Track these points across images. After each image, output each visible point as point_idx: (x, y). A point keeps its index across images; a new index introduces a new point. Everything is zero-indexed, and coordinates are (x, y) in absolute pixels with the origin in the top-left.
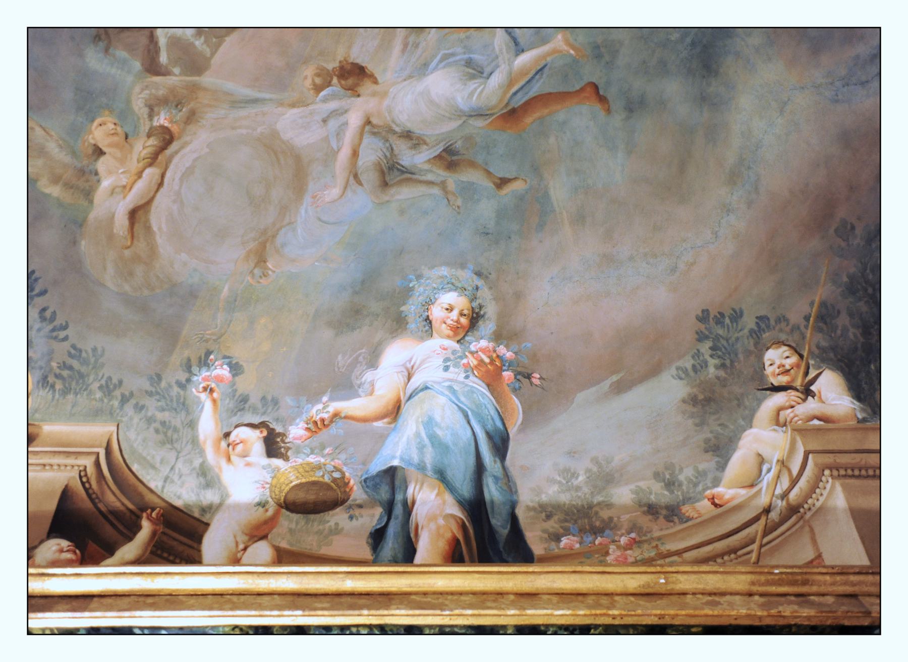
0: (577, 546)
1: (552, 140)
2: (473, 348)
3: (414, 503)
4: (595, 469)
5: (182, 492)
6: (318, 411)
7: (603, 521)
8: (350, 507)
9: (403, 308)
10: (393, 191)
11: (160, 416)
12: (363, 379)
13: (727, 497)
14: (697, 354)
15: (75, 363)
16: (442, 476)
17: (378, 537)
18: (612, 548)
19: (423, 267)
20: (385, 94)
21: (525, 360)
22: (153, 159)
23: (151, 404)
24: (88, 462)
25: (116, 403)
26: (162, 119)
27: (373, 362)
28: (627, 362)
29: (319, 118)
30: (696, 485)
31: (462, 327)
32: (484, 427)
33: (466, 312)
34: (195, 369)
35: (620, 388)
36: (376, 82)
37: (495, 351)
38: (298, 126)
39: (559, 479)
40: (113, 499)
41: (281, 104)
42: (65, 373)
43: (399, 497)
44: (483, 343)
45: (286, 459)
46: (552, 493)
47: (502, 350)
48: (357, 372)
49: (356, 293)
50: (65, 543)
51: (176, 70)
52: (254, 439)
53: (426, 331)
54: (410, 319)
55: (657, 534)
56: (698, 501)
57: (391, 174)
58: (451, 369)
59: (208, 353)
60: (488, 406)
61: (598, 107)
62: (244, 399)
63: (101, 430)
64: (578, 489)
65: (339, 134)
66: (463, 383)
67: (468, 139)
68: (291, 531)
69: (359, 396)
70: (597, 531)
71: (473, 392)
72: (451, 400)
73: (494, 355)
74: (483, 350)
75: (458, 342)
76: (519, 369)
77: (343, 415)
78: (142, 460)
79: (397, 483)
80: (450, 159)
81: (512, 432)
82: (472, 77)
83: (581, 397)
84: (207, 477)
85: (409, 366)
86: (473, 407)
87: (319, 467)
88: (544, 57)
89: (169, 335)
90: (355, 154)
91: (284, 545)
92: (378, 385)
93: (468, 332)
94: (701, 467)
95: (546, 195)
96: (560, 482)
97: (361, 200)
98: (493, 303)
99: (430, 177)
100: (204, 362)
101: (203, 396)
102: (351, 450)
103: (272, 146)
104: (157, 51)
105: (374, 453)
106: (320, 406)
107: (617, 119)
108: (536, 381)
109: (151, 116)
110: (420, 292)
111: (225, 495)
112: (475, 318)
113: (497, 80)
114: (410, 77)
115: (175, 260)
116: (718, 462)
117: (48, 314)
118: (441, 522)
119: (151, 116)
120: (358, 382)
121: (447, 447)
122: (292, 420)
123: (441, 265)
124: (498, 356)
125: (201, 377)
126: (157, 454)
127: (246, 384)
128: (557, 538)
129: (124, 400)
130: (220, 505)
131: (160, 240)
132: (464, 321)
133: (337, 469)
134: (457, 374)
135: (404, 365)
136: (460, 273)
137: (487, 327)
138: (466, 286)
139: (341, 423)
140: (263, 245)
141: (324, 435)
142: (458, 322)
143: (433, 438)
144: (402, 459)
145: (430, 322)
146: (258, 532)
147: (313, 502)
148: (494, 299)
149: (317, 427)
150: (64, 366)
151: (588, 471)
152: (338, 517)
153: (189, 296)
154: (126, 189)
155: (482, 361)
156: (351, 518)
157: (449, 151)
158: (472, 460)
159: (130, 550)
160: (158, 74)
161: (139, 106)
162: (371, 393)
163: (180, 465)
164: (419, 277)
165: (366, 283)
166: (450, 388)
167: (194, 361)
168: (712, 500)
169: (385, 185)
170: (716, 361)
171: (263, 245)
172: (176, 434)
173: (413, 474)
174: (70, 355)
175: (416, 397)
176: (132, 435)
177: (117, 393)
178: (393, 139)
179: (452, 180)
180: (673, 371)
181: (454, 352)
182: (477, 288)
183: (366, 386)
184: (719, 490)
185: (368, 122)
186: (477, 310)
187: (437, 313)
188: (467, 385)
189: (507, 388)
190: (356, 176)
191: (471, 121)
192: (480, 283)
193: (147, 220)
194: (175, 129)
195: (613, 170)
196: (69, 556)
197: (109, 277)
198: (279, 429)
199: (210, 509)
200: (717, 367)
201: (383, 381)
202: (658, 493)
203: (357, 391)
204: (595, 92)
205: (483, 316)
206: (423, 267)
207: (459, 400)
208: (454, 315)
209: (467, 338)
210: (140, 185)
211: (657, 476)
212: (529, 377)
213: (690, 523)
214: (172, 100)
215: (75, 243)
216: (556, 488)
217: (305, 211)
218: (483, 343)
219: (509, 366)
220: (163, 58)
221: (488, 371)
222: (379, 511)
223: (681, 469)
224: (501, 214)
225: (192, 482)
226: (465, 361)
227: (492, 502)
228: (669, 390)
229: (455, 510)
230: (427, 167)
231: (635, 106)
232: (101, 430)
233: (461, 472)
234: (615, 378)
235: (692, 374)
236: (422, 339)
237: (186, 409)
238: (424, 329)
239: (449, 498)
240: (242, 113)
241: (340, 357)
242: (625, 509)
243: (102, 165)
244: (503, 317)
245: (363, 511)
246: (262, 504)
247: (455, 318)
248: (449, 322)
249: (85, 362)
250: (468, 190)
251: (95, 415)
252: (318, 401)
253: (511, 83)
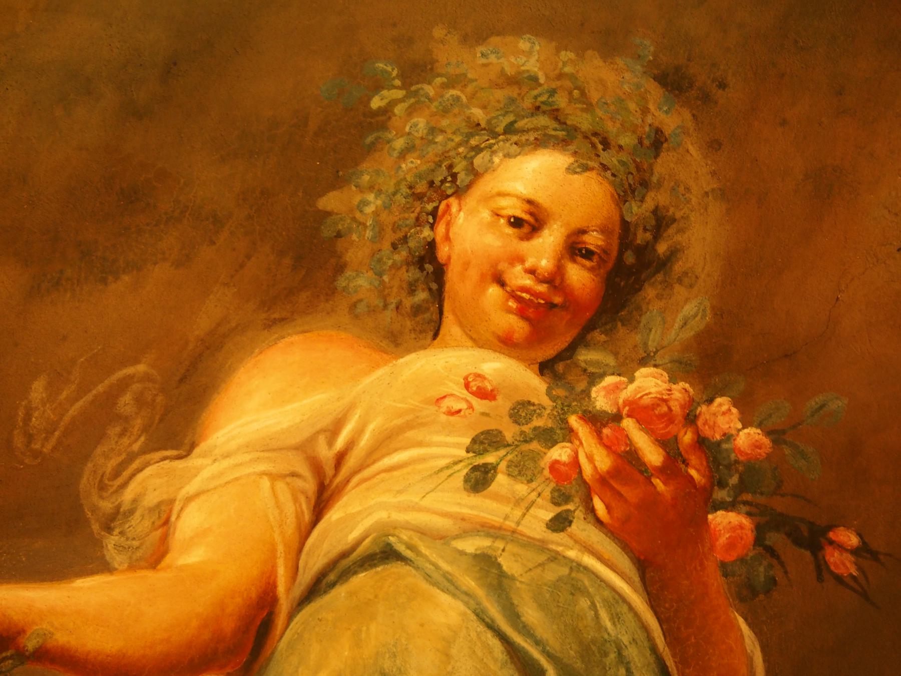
9: (330, 201)
12: (128, 495)
19: (438, 32)
27: (176, 424)
31: (571, 302)
33: (594, 240)
37: (691, 419)
44: (649, 382)
47: (722, 416)
48: (104, 460)
53: (417, 310)
54: (357, 251)
58: (501, 480)
60: (632, 653)
66: (541, 546)
69: (106, 568)
71: (577, 590)
72: (481, 615)
73: (687, 437)
74: (641, 412)
75: (545, 368)
76: (780, 505)
77: (31, 644)
85: (326, 454)
86: (571, 654)
92: (189, 522)
93: (590, 327)
98: (716, 209)
108: (841, 562)
110: (413, 130)
112: (624, 272)
120: (106, 506)
123: (518, 30)
124: (701, 442)
134: (519, 506)
135: (305, 448)
137: (679, 313)
138: (611, 128)
142: (555, 280)
145: (439, 273)
148: (723, 194)
155: (629, 458)
162: (156, 558)
164: (417, 71)
166: (485, 563)
175: (341, 592)
181: (522, 410)
182: (657, 142)
183: (139, 525)
186: (642, 237)
187: (471, 232)
188: (555, 557)
189: (716, 582)
192: (671, 119)
203: (98, 544)
205: (664, 264)
206: (438, 32)
207: (514, 617)
208: (544, 249)
209: (585, 356)
212: (814, 540)
218: (649, 382)
219: (743, 486)
221: (651, 502)
226: (560, 453)
236: (395, 343)
238: (408, 302)
241: (38, 390)
247: (545, 264)
248: (519, 278)
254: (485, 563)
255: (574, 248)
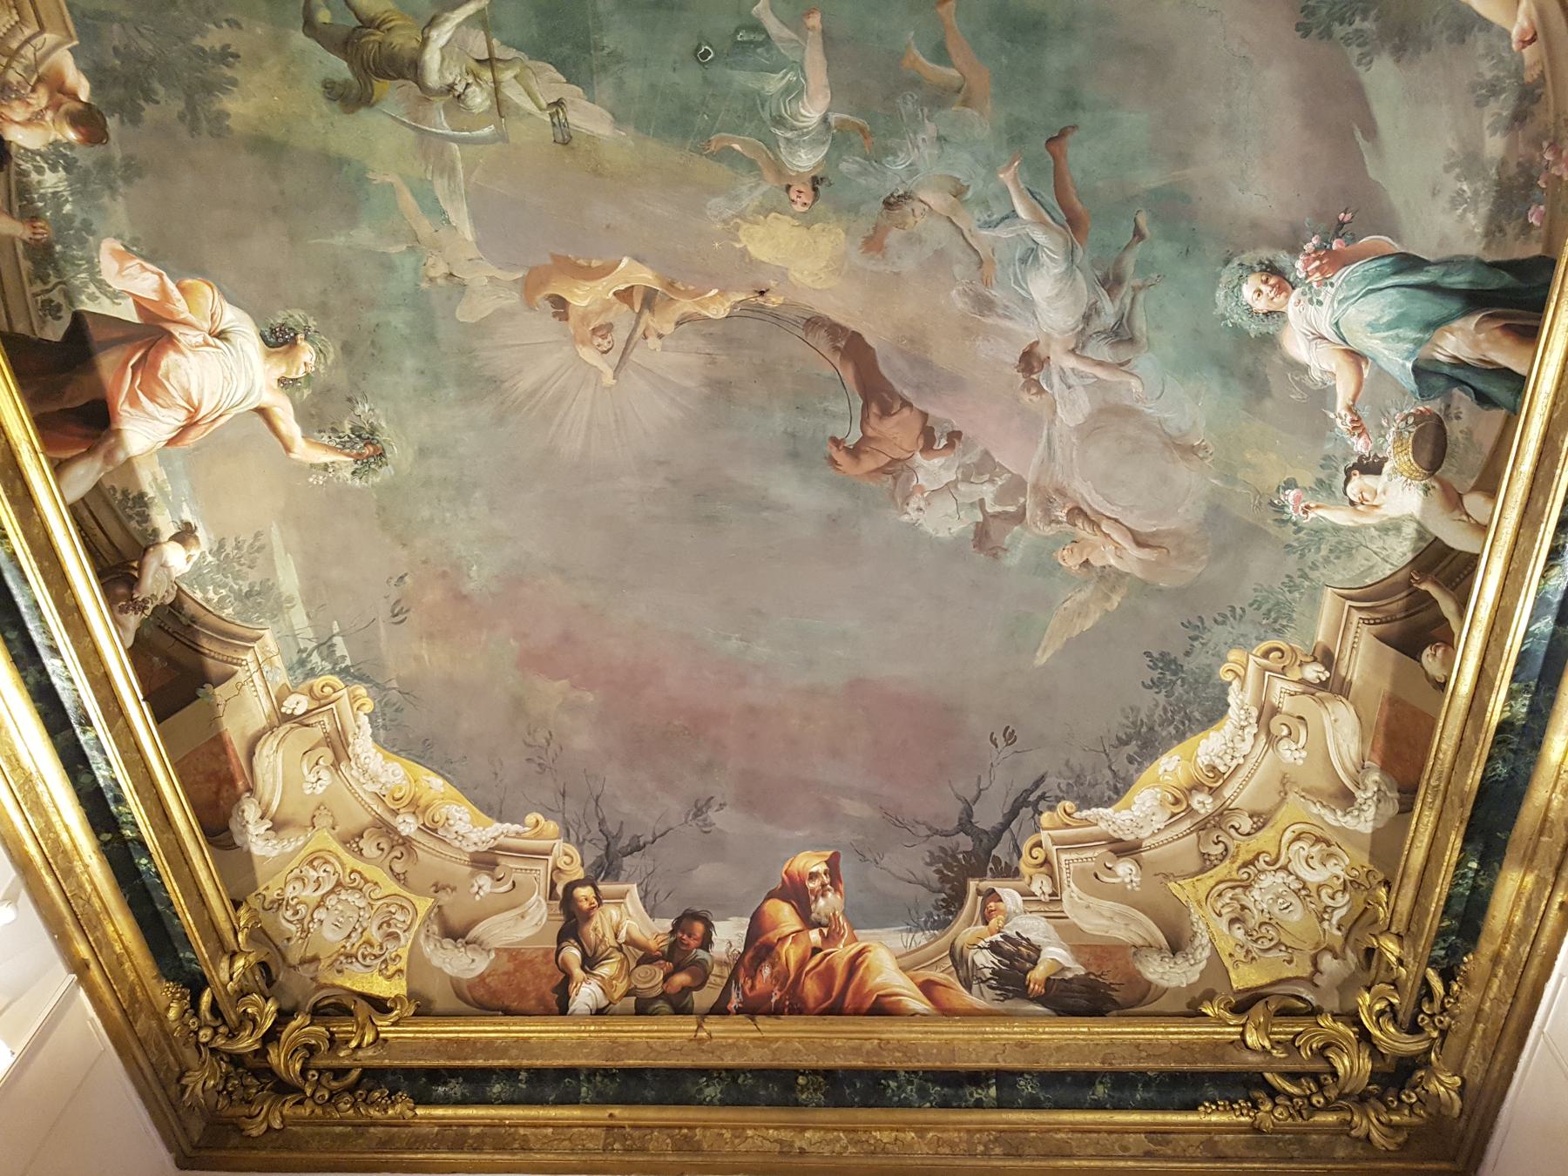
0: (1542, 208)
1: (1100, 184)
2: (1303, 275)
3: (1455, 358)
4: (1457, 170)
5: (1401, 551)
6: (1343, 423)
7: (1520, 174)
8: (1447, 416)
10: (1138, 334)
11: (1324, 552)
13: (1526, 24)
14: (1347, 40)
15: (1264, 608)
16: (1432, 326)
17: (1483, 399)
18: (1554, 171)
20: (1048, 335)
21: (1323, 226)
22: (1095, 525)
23: (1311, 557)
24: (1356, 616)
25: (1307, 583)
26: (1062, 514)
27: (1305, 369)
28: (1341, 119)
29: (1067, 392)
30: (1502, 59)
32: (1388, 276)
34: (1285, 517)
35: (1371, 131)
36: (1037, 343)
38: (1072, 410)
39: (1460, 211)
40: (1396, 605)
41: (1052, 422)
42: (1273, 615)
43: (1446, 370)
44: (1299, 264)
45: (1386, 459)
46: (1475, 221)
47: (1308, 247)
49: (1232, 375)
50: (1428, 651)
51: (1022, 500)
52: (1358, 483)
55: (1551, 117)
56: (1522, 61)
57: (1122, 334)
59: (1272, 504)
61: (1069, 138)
62: (1320, 482)
63: (1329, 600)
64: (1476, 192)
65: (1081, 375)
67: (1093, 264)
68: (1459, 472)
70: (1531, 183)
74: (1306, 267)
78: (1364, 574)
79: (1431, 368)
80: (1111, 282)
81: (1398, 248)
82: (1036, 258)
83: (1372, 174)
84: (1391, 528)
87: (1399, 433)
88: (1020, 191)
89: (1252, 533)
90: (1100, 364)
91: (1472, 482)
92: (1326, 367)
94: (1481, 49)
95: (1154, 191)
96: (1465, 210)
97: (1144, 362)
99: (1128, 301)
100: (1281, 509)
101: (1311, 515)
102: (1388, 402)
103: (1089, 431)
104: (1006, 513)
105: (1395, 382)
106: (1339, 421)
107: (1084, 118)
109: (1059, 522)
111: (1412, 518)
113: (1040, 236)
114: (1034, 314)
115: (1184, 516)
116: (1480, 30)
117: (1220, 619)
118: (1482, 336)
119: (1059, 522)
121: (1402, 315)
122: (1349, 450)
125: (1292, 513)
126: (1360, 562)
127: (1306, 478)
128: (1528, 227)
129: (1305, 576)
130: (1419, 523)
131: (1164, 528)
132: (1272, 281)
133: (1405, 418)
134: (1327, 294)
136: (1223, 280)
137: (1283, 259)
139: (1358, 406)
140: (1178, 447)
141: (1368, 423)
142: (1273, 286)
143: (1390, 326)
144: (1407, 359)
146: (1454, 501)
147: (1433, 448)
149: (1358, 427)
150: (1267, 614)
151: (1458, 178)
152: (1454, 429)
153: (1216, 512)
154: (1118, 547)
155: (1317, 268)
156: (1458, 418)
157: (1103, 283)
158: (1423, 294)
159: (1447, 607)
160: (1024, 514)
161: (1050, 531)
163: (1374, 547)
164: (1224, 318)
165: (1224, 366)
167: (1277, 516)
168: (1524, 44)
169: (1132, 340)
170: (1358, 19)
171: (1178, 447)
172: (1344, 544)
173: (1423, 352)
174: (1258, 609)
176: (1338, 577)
177: (1298, 581)
178: (1089, 331)
179: (1131, 281)
180: (1361, 69)
181: (1304, 294)
184: (1515, 33)
185: (1073, 351)
187: (1261, 305)
190: (1121, 365)
191: (1078, 261)
192: (1236, 262)
193: (1147, 534)
194: (1070, 505)
195: (1135, 122)
196: (1440, 652)
197: (1193, 570)
198: (1355, 460)
199: (1422, 532)
200: (1363, 19)
201: (1323, 362)
202: (1502, 107)
204: (1055, 141)
208: (1264, 288)
210: (1115, 536)
211: (1481, 103)
212: (1342, 224)
213: (1548, 76)
214: (1046, 506)
215: (1160, 590)
216: (1470, 216)
217: (1150, 409)
218: (1299, 264)
220: (1012, 509)
222: (1456, 391)
223: (1480, 74)
224: (1168, 237)
225: (1391, 540)
227: (1471, 282)
228: (1383, 78)
229: (1474, 320)
230: (1117, 303)
231: (1071, 101)
232: (1329, 600)
233: (1431, 307)
234: (1358, 134)
235: (1367, 48)
236: (1285, 322)
237: (1319, 532)
239: (1457, 324)
240: (1059, 452)
242: (1511, 147)
243: (1097, 562)
244: (1276, 243)
245: (1454, 404)
246: (1427, 490)
249: (1266, 599)
250: (1143, 267)
251: (1314, 601)
252: (1333, 421)
253: (1043, 223)
254: (1340, 302)
255: (1266, 282)
